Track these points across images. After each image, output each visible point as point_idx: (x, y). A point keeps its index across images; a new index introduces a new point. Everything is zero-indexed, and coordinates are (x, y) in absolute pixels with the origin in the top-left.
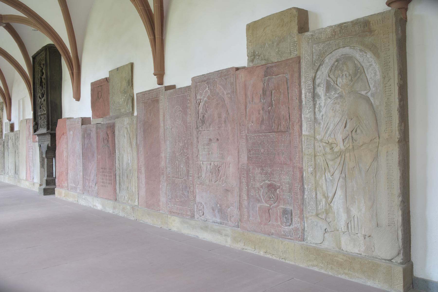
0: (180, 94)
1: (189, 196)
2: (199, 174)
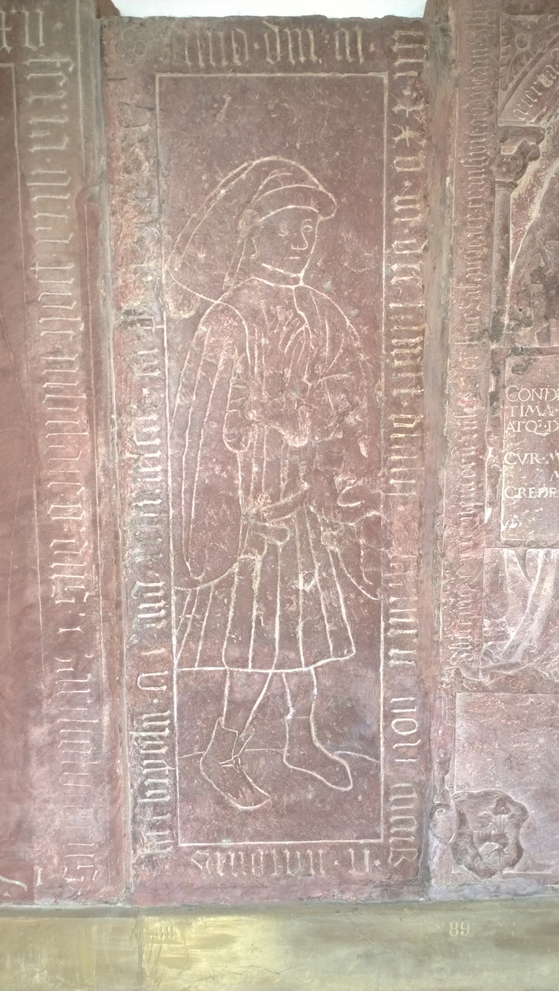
0: (308, 66)
1: (378, 767)
2: (487, 622)
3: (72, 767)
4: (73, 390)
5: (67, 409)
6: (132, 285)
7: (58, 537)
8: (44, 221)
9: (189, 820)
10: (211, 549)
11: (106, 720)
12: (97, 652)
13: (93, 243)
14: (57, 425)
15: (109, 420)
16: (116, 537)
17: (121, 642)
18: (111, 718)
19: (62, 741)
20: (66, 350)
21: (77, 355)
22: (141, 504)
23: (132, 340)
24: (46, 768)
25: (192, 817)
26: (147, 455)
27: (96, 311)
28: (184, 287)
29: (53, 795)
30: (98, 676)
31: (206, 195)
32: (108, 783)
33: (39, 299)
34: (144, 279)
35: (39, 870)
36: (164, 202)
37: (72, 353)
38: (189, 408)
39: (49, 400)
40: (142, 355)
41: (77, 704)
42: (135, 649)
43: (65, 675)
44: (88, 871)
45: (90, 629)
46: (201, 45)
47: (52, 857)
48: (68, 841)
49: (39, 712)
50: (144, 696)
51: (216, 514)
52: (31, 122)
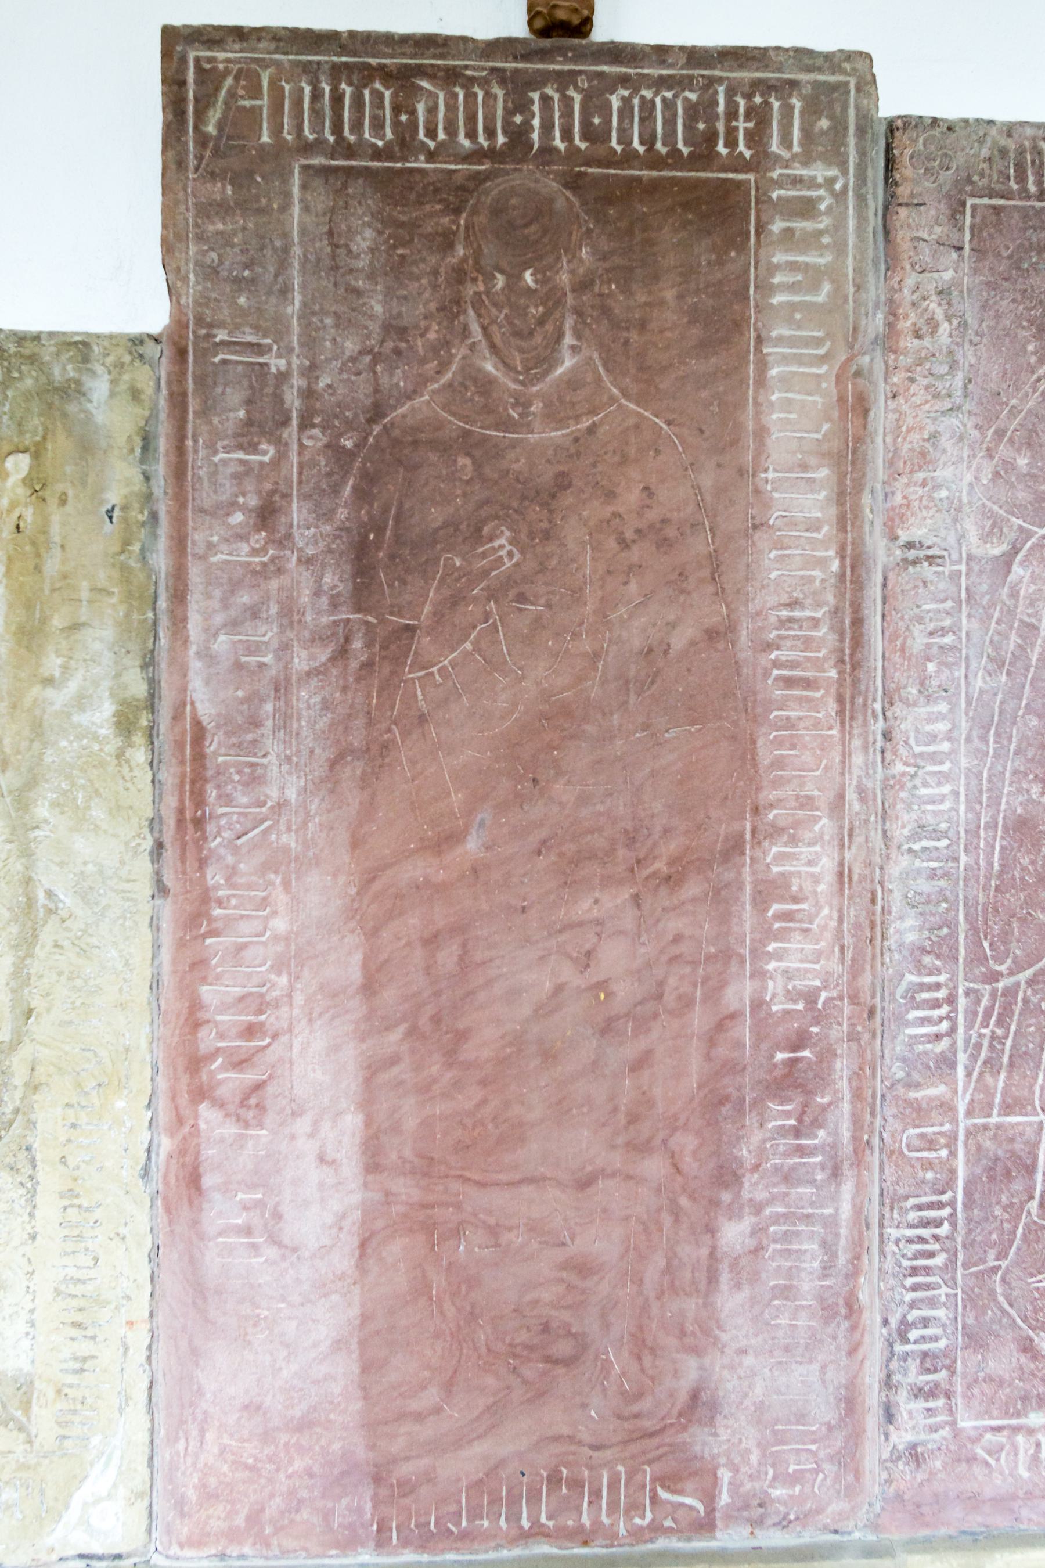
3: (786, 1292)
4: (818, 664)
5: (805, 693)
6: (916, 504)
7: (782, 899)
8: (788, 405)
9: (976, 1381)
10: (1023, 920)
11: (846, 1210)
12: (836, 1092)
13: (859, 440)
14: (788, 718)
15: (870, 711)
16: (873, 901)
17: (874, 1076)
18: (854, 1206)
19: (773, 1246)
20: (808, 602)
21: (825, 609)
22: (916, 847)
23: (916, 587)
24: (745, 1293)
25: (981, 1375)
26: (930, 768)
27: (858, 543)
28: (996, 508)
29: (753, 1341)
30: (836, 1134)
31: (1033, 372)
32: (846, 1317)
33: (771, 522)
34: (935, 495)
35: (725, 1475)
36: (970, 381)
37: (818, 605)
38: (996, 694)
39: (778, 678)
40: (928, 611)
41: (800, 1182)
42: (899, 1087)
43: (782, 1132)
44: (808, 1475)
45: (827, 1055)
46: (1033, 162)
47: (748, 1451)
48: (777, 1421)
49: (738, 1195)
50: (913, 1167)
51: (1033, 862)
52: (775, 260)
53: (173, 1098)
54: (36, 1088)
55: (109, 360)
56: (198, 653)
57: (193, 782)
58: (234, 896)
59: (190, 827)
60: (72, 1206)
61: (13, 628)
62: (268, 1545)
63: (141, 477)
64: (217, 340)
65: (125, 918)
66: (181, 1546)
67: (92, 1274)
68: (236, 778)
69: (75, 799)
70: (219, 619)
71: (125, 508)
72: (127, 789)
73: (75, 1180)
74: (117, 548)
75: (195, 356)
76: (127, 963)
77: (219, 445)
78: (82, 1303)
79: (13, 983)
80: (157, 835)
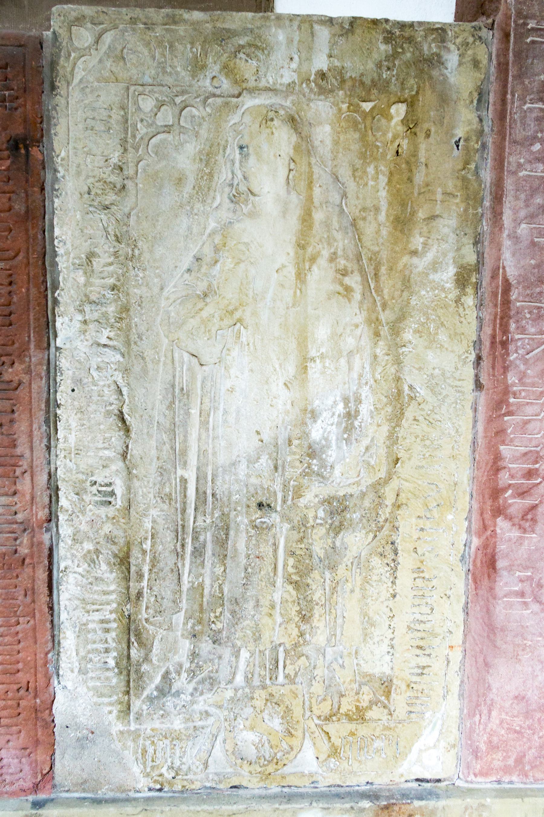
53: (482, 514)
54: (399, 506)
55: (458, 41)
56: (509, 236)
57: (502, 318)
58: (524, 390)
59: (499, 347)
60: (419, 577)
61: (392, 218)
62: (527, 776)
63: (477, 119)
64: (529, 27)
65: (456, 403)
66: (475, 775)
67: (430, 618)
68: (528, 316)
69: (429, 328)
70: (522, 213)
71: (467, 140)
72: (461, 322)
73: (422, 562)
74: (460, 167)
75: (515, 38)
76: (457, 431)
77: (528, 98)
78: (422, 634)
79: (388, 443)
80: (477, 352)
